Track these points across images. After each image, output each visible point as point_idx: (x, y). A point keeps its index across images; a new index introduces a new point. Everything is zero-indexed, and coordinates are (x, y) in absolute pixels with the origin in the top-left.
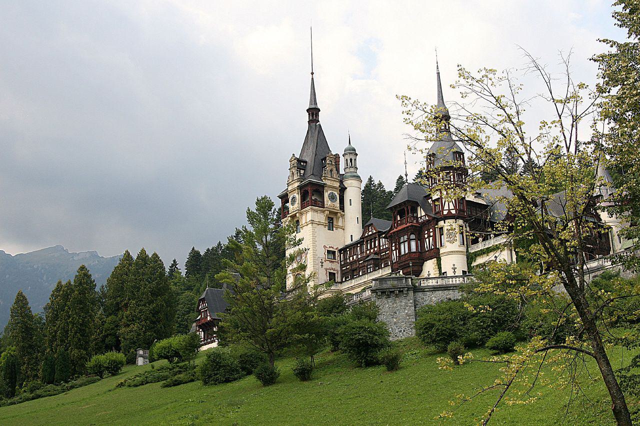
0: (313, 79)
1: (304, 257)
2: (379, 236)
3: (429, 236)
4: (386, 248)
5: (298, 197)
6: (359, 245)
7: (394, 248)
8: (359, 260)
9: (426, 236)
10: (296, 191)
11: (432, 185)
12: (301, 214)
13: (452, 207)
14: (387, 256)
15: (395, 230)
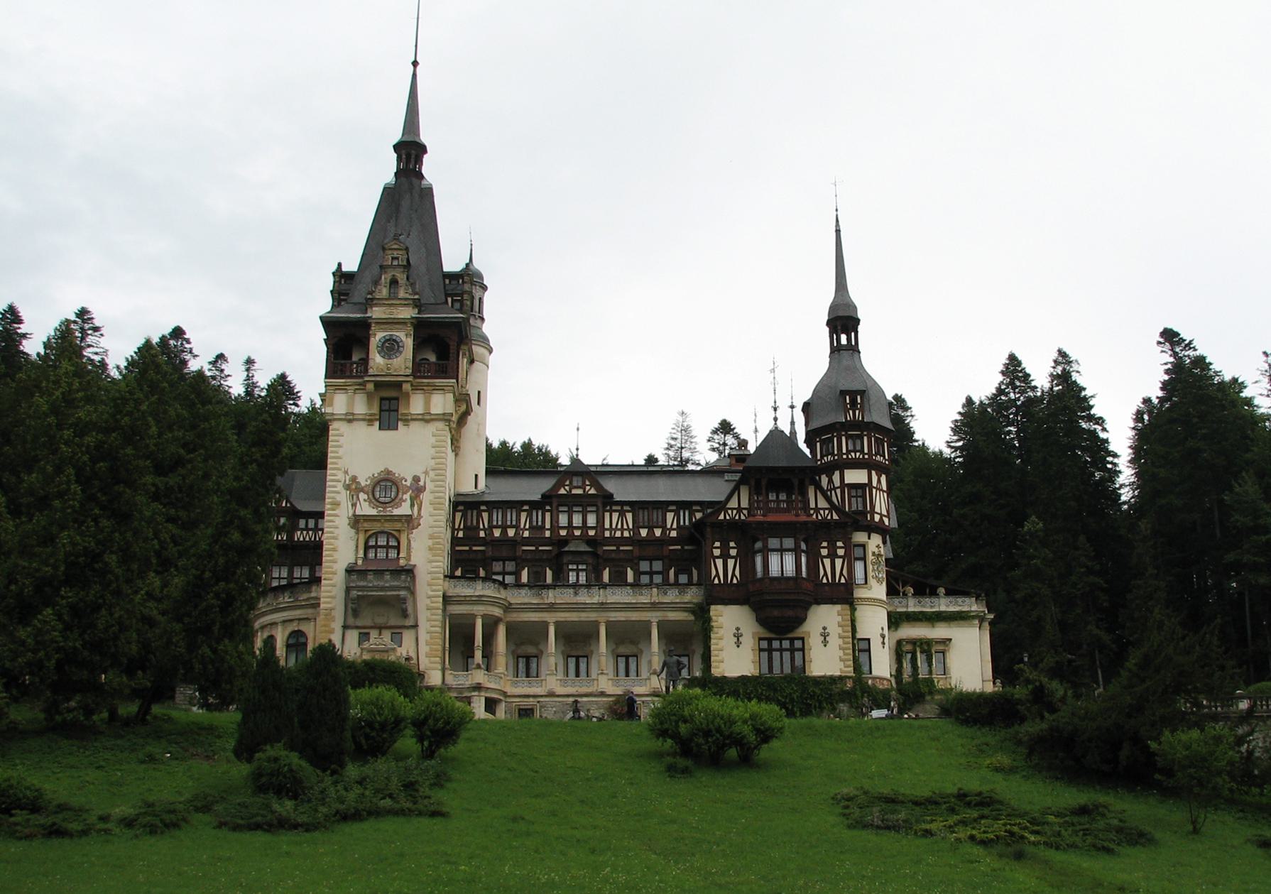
0: (414, 75)
1: (407, 497)
2: (605, 505)
3: (833, 556)
4: (622, 537)
5: (409, 343)
6: (526, 507)
7: (717, 552)
8: (527, 542)
9: (824, 552)
10: (411, 330)
11: (848, 452)
12: (416, 388)
13: (884, 512)
14: (622, 555)
15: (760, 518)
